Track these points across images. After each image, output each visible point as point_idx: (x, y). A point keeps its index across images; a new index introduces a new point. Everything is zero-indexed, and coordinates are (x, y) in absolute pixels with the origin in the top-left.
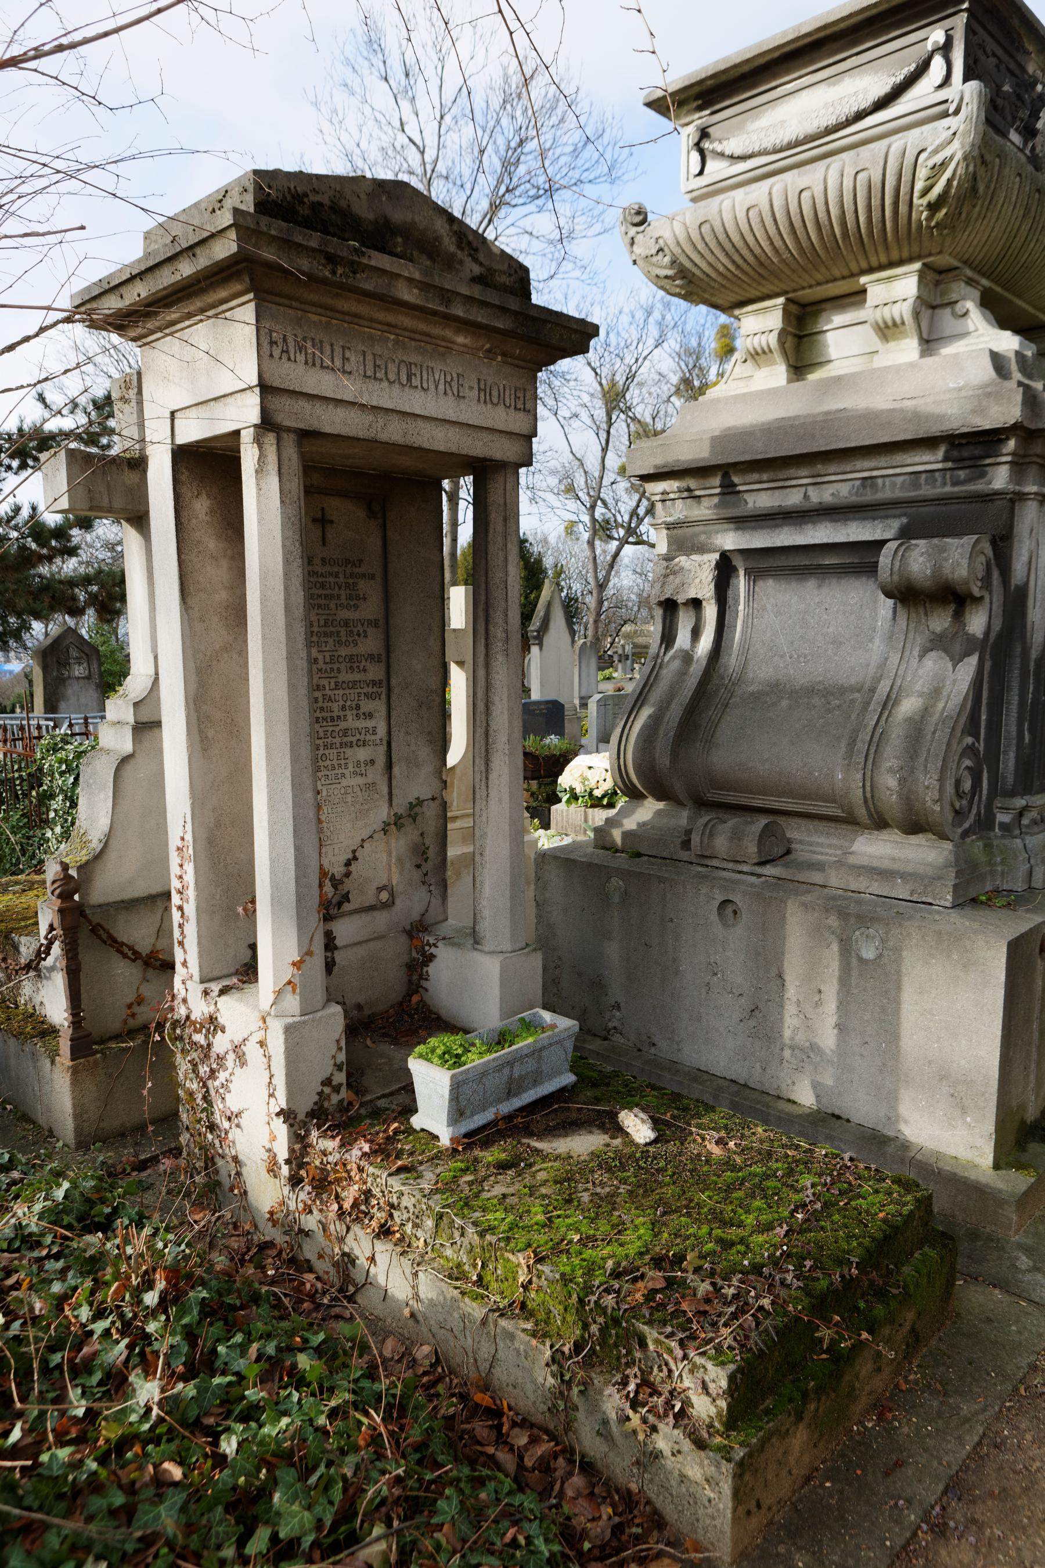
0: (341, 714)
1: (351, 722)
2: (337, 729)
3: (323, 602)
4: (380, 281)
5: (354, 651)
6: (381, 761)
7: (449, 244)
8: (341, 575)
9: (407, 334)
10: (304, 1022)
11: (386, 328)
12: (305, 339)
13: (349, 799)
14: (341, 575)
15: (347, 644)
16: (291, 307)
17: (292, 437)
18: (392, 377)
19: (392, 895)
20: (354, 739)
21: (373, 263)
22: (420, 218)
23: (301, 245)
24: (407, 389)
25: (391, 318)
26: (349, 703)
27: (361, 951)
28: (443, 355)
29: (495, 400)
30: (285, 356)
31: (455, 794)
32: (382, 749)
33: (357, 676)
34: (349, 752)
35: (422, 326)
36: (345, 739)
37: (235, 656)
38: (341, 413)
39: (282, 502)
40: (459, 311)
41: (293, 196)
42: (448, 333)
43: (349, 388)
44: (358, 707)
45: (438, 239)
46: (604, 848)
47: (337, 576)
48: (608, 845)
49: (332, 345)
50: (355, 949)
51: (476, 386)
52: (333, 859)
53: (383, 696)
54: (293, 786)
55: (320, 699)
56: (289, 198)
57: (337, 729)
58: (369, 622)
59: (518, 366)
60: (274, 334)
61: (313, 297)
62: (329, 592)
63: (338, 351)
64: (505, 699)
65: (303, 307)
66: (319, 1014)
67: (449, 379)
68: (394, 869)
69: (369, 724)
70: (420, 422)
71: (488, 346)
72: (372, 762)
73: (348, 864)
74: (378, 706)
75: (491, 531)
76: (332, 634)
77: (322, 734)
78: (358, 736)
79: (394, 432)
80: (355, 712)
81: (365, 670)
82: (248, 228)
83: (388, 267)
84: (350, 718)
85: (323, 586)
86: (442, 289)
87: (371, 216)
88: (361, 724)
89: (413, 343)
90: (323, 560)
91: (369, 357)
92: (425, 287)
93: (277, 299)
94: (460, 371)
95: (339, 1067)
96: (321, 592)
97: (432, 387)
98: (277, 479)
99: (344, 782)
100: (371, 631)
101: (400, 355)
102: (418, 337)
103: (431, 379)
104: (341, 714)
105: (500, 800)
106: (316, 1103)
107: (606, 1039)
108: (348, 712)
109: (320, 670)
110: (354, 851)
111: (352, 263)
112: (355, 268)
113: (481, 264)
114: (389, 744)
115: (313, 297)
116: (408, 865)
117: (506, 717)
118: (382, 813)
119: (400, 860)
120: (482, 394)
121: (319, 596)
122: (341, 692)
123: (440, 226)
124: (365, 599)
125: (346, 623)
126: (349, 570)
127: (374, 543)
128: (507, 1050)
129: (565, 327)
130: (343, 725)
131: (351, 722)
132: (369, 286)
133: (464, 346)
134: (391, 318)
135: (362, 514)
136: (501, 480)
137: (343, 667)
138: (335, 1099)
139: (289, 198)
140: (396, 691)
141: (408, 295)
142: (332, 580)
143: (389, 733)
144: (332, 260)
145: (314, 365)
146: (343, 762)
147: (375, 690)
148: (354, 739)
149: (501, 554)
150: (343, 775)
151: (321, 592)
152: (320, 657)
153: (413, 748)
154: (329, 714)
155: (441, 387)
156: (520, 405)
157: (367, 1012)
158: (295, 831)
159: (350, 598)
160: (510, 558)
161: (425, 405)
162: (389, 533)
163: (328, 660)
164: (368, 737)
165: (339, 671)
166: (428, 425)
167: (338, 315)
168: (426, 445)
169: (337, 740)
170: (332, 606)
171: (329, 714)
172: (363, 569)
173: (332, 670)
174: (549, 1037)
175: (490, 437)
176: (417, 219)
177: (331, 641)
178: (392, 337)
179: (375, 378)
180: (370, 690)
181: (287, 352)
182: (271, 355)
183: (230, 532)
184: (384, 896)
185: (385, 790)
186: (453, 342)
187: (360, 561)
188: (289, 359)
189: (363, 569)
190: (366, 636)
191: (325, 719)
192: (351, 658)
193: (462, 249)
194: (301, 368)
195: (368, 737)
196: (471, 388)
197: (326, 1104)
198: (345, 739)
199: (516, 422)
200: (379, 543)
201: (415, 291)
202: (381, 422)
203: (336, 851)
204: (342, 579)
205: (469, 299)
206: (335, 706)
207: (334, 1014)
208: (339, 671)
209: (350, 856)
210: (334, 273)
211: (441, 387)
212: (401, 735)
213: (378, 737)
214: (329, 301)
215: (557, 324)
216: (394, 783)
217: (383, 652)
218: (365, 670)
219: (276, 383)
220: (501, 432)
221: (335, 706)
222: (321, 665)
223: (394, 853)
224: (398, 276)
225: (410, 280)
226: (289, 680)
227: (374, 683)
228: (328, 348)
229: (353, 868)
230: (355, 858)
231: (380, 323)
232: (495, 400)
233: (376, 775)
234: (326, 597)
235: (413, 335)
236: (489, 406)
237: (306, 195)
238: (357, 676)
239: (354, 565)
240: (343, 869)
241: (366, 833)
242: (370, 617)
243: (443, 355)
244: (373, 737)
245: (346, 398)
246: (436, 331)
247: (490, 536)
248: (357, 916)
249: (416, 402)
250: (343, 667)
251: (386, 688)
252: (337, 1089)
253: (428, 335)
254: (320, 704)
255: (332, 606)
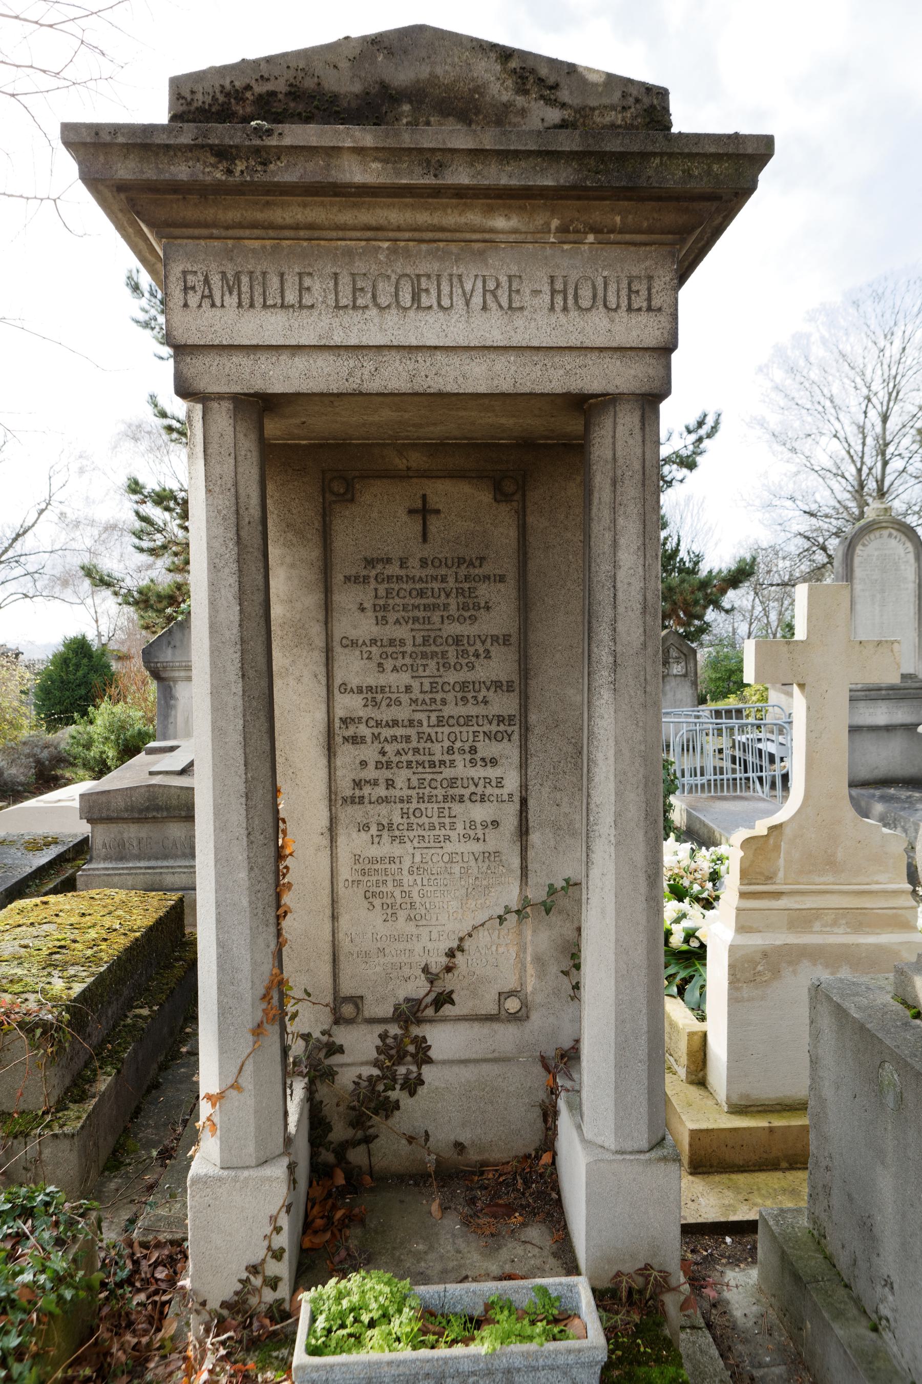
0: (447, 758)
1: (461, 769)
2: (439, 778)
3: (420, 614)
4: (310, 166)
5: (470, 676)
6: (510, 822)
7: (500, 90)
8: (451, 580)
9: (407, 235)
10: (220, 1179)
11: (369, 234)
12: (237, 276)
13: (456, 869)
14: (451, 580)
15: (457, 667)
16: (211, 237)
17: (227, 405)
18: (383, 300)
19: (524, 1004)
20: (466, 793)
21: (287, 141)
22: (445, 70)
23: (167, 147)
24: (411, 313)
25: (365, 217)
26: (458, 744)
27: (467, 1074)
28: (481, 253)
29: (585, 303)
30: (206, 303)
31: (781, 862)
32: (513, 808)
33: (472, 710)
34: (457, 808)
35: (423, 218)
36: (451, 792)
37: (292, 683)
38: (300, 362)
39: (208, 491)
40: (461, 176)
41: (228, 95)
42: (473, 217)
43: (308, 329)
44: (473, 750)
45: (479, 89)
46: (904, 1002)
47: (444, 579)
48: (910, 1002)
49: (282, 275)
50: (456, 1069)
51: (546, 288)
52: (430, 946)
53: (516, 737)
54: (216, 861)
55: (414, 738)
56: (221, 98)
57: (439, 778)
58: (495, 639)
59: (634, 244)
60: (190, 277)
61: (232, 215)
62: (431, 601)
63: (291, 281)
64: (612, 759)
65: (231, 233)
66: (246, 1173)
67: (491, 285)
68: (530, 970)
69: (492, 773)
70: (439, 356)
71: (555, 223)
72: (495, 824)
73: (451, 954)
74: (509, 751)
75: (595, 501)
76: (434, 654)
77: (415, 783)
78: (472, 788)
79: (394, 376)
80: (468, 757)
81: (486, 702)
82: (84, 144)
83: (314, 142)
84: (460, 764)
85: (421, 593)
86: (421, 150)
87: (357, 88)
88: (478, 772)
89: (424, 247)
90: (424, 563)
91: (345, 281)
92: (390, 155)
93: (189, 232)
94: (514, 270)
95: (277, 1255)
96: (418, 601)
97: (459, 302)
98: (202, 462)
99: (449, 847)
100: (494, 650)
101: (400, 266)
102: (429, 235)
103: (458, 291)
104: (447, 758)
105: (603, 912)
106: (237, 1293)
107: (875, 1329)
108: (457, 757)
109: (415, 701)
110: (461, 939)
111: (257, 151)
112: (263, 156)
113: (563, 105)
114: (524, 802)
115: (232, 215)
116: (554, 969)
117: (612, 785)
118: (509, 893)
119: (538, 960)
120: (559, 299)
121: (417, 607)
122: (447, 730)
123: (486, 71)
124: (488, 608)
125: (457, 640)
126: (463, 571)
127: (504, 533)
128: (443, 1352)
129: (691, 156)
130: (448, 773)
131: (461, 769)
132: (290, 176)
133: (515, 231)
134: (365, 217)
135: (485, 497)
136: (608, 422)
137: (450, 697)
138: (269, 1296)
139: (221, 98)
140: (537, 731)
141: (357, 173)
142: (436, 585)
143: (524, 787)
144: (223, 154)
145: (252, 305)
146: (447, 821)
147: (502, 728)
148: (466, 793)
149: (608, 536)
150: (448, 838)
151: (418, 601)
152: (416, 685)
153: (565, 808)
154: (427, 758)
155: (477, 300)
156: (639, 302)
157: (473, 1156)
158: (218, 921)
159: (465, 608)
160: (622, 541)
161: (471, 328)
162: (530, 519)
163: (427, 687)
164: (489, 791)
165: (444, 702)
166: (455, 360)
167: (287, 233)
168: (452, 388)
169: (440, 792)
170: (436, 618)
171: (427, 758)
172: (486, 569)
173: (433, 701)
174: (526, 1355)
175: (579, 361)
176: (439, 71)
177: (432, 664)
178: (386, 245)
179: (355, 307)
180: (494, 728)
181: (211, 296)
182: (186, 305)
183: (290, 536)
184: (512, 1005)
185: (516, 862)
186: (492, 231)
187: (482, 559)
188: (213, 305)
189: (486, 569)
190: (488, 656)
191: (420, 764)
192: (464, 685)
193: (526, 92)
194: (231, 313)
195: (489, 791)
196: (536, 293)
197: (253, 1301)
198: (451, 792)
199: (641, 330)
200: (513, 533)
201: (374, 165)
202: (369, 366)
203: (434, 936)
204: (451, 583)
205: (477, 155)
206: (437, 748)
207: (269, 1179)
208: (444, 702)
209: (455, 944)
210: (229, 172)
211: (477, 300)
212: (546, 790)
213: (505, 791)
214: (259, 216)
215: (671, 155)
216: (531, 854)
217: (515, 678)
218: (486, 702)
219: (194, 339)
220: (601, 349)
221: (437, 748)
222: (416, 693)
223: (529, 950)
224: (336, 150)
225: (359, 151)
226: (214, 723)
227: (500, 719)
228: (274, 282)
229: (460, 958)
230: (460, 949)
231: (354, 228)
232: (612, 301)
233: (503, 840)
234: (426, 607)
235: (417, 235)
236: (574, 314)
237: (248, 87)
238: (472, 710)
239: (471, 564)
240: (444, 960)
241: (481, 917)
242: (495, 632)
243: (481, 253)
244: (498, 791)
245: (303, 341)
246: (451, 219)
247: (594, 510)
248: (466, 1025)
249: (428, 328)
250: (450, 697)
251: (521, 726)
252: (273, 1283)
253: (442, 229)
254: (414, 744)
255: (436, 618)
